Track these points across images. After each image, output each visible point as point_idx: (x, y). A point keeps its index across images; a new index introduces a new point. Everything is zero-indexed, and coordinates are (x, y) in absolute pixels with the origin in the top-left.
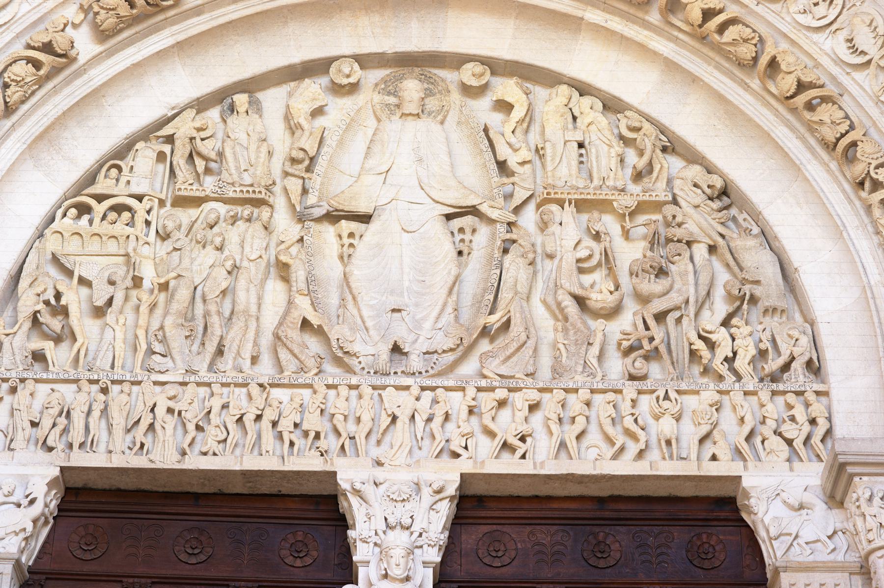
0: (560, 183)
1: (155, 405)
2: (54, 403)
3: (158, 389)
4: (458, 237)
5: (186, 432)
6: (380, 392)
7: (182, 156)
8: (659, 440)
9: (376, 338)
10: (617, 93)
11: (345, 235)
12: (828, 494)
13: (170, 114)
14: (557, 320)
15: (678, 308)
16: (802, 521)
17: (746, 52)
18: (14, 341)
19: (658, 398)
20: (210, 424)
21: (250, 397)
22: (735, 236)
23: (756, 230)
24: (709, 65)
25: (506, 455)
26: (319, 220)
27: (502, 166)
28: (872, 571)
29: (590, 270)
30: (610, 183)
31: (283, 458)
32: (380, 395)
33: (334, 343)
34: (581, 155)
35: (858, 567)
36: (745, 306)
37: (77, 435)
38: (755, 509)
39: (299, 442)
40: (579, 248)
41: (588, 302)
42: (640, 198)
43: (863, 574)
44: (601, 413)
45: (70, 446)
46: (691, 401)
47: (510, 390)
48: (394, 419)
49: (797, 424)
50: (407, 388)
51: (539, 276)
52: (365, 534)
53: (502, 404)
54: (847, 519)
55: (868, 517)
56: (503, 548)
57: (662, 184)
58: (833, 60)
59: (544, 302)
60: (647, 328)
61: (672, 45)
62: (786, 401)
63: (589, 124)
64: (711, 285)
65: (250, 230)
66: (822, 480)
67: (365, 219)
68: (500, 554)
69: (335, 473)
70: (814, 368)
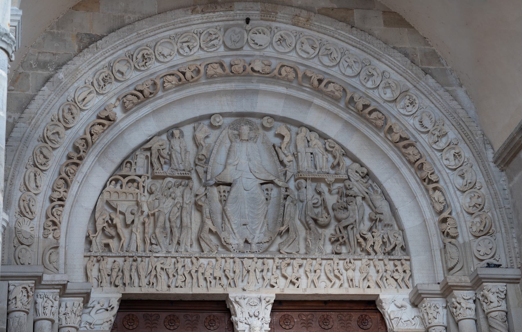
0: (304, 170)
1: (156, 267)
2: (116, 266)
3: (156, 259)
4: (266, 192)
5: (169, 278)
6: (242, 260)
7: (155, 158)
8: (348, 280)
9: (238, 237)
10: (325, 132)
11: (222, 191)
13: (148, 139)
14: (306, 229)
15: (352, 224)
17: (380, 123)
18: (97, 240)
19: (347, 262)
20: (178, 274)
21: (192, 263)
22: (372, 193)
23: (379, 191)
24: (363, 124)
25: (291, 286)
26: (211, 186)
27: (282, 162)
29: (317, 207)
30: (324, 170)
31: (207, 287)
32: (242, 262)
33: (223, 240)
34: (311, 157)
36: (377, 223)
37: (127, 280)
38: (385, 307)
39: (213, 282)
40: (313, 199)
41: (318, 222)
42: (337, 177)
44: (326, 268)
45: (124, 284)
46: (358, 263)
47: (291, 259)
48: (248, 272)
49: (399, 273)
50: (252, 258)
51: (297, 209)
52: (242, 319)
53: (289, 264)
55: (429, 314)
56: (289, 322)
57: (343, 171)
58: (413, 128)
59: (300, 220)
60: (340, 231)
61: (348, 115)
63: (315, 145)
64: (364, 213)
65: (186, 191)
67: (230, 185)
68: (288, 324)
69: (228, 294)
70: (404, 249)
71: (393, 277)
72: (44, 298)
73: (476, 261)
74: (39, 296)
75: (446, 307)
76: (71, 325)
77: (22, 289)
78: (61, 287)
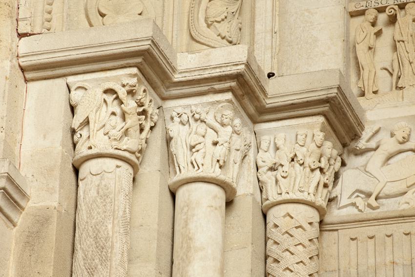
72: (191, 121)
74: (177, 119)
76: (292, 196)
77: (105, 96)
78: (233, 84)
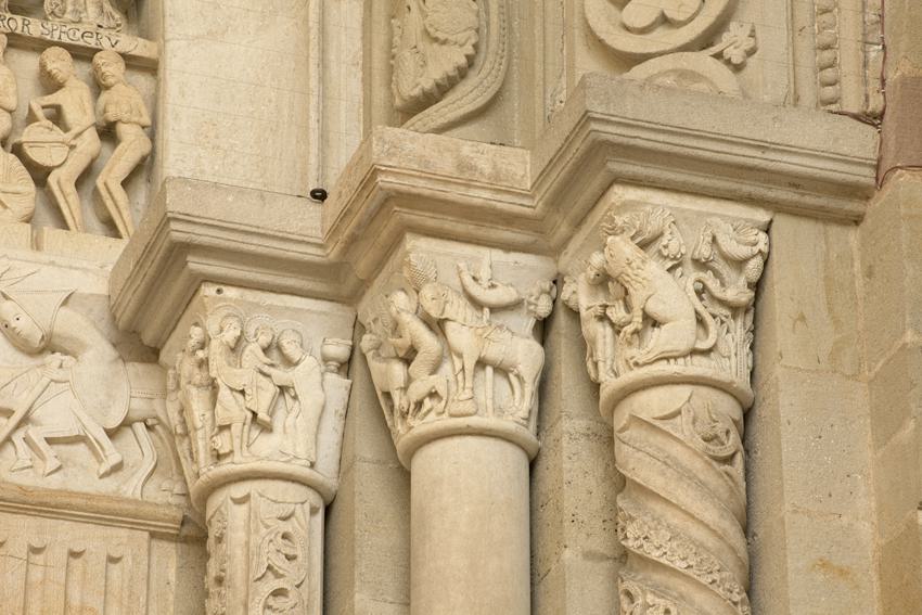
12: (124, 318)
16: (46, 380)
28: (213, 533)
35: (173, 520)
43: (185, 540)
54: (164, 394)
62: (43, 66)
66: (112, 282)
71: (18, 150)
73: (588, 63)
75: (345, 367)
